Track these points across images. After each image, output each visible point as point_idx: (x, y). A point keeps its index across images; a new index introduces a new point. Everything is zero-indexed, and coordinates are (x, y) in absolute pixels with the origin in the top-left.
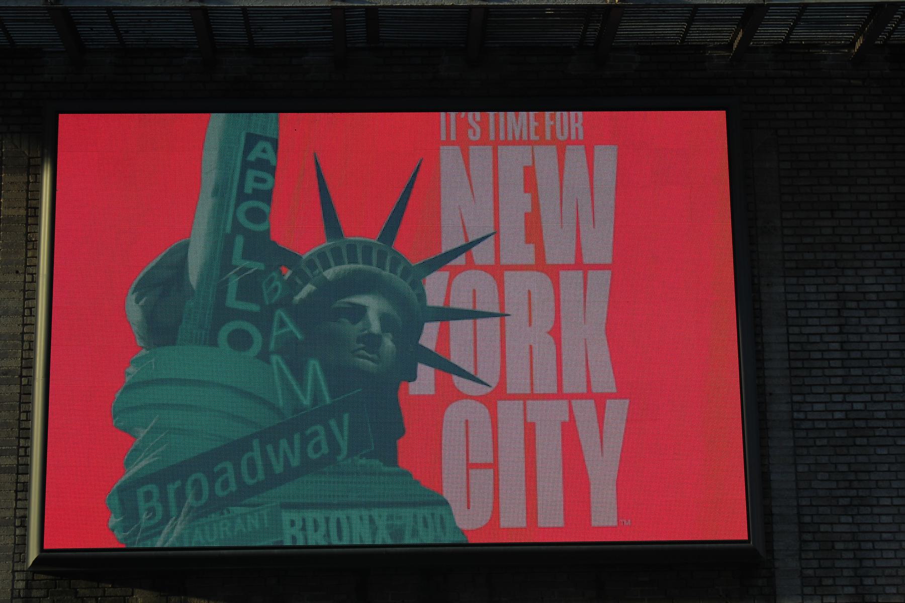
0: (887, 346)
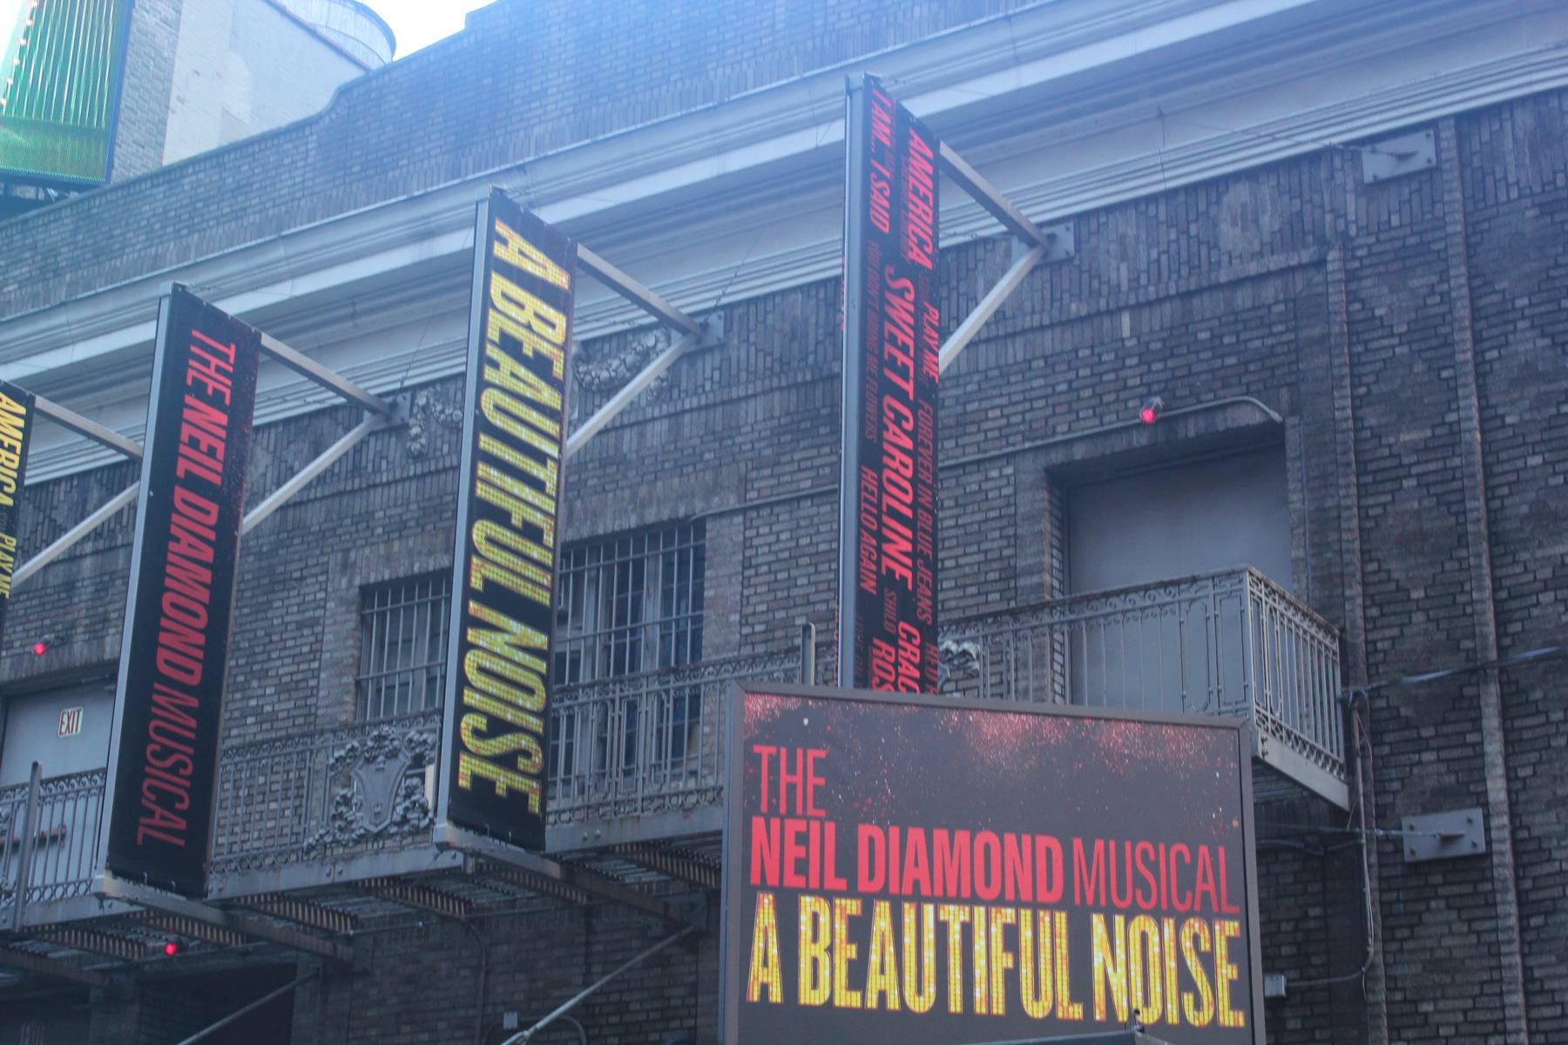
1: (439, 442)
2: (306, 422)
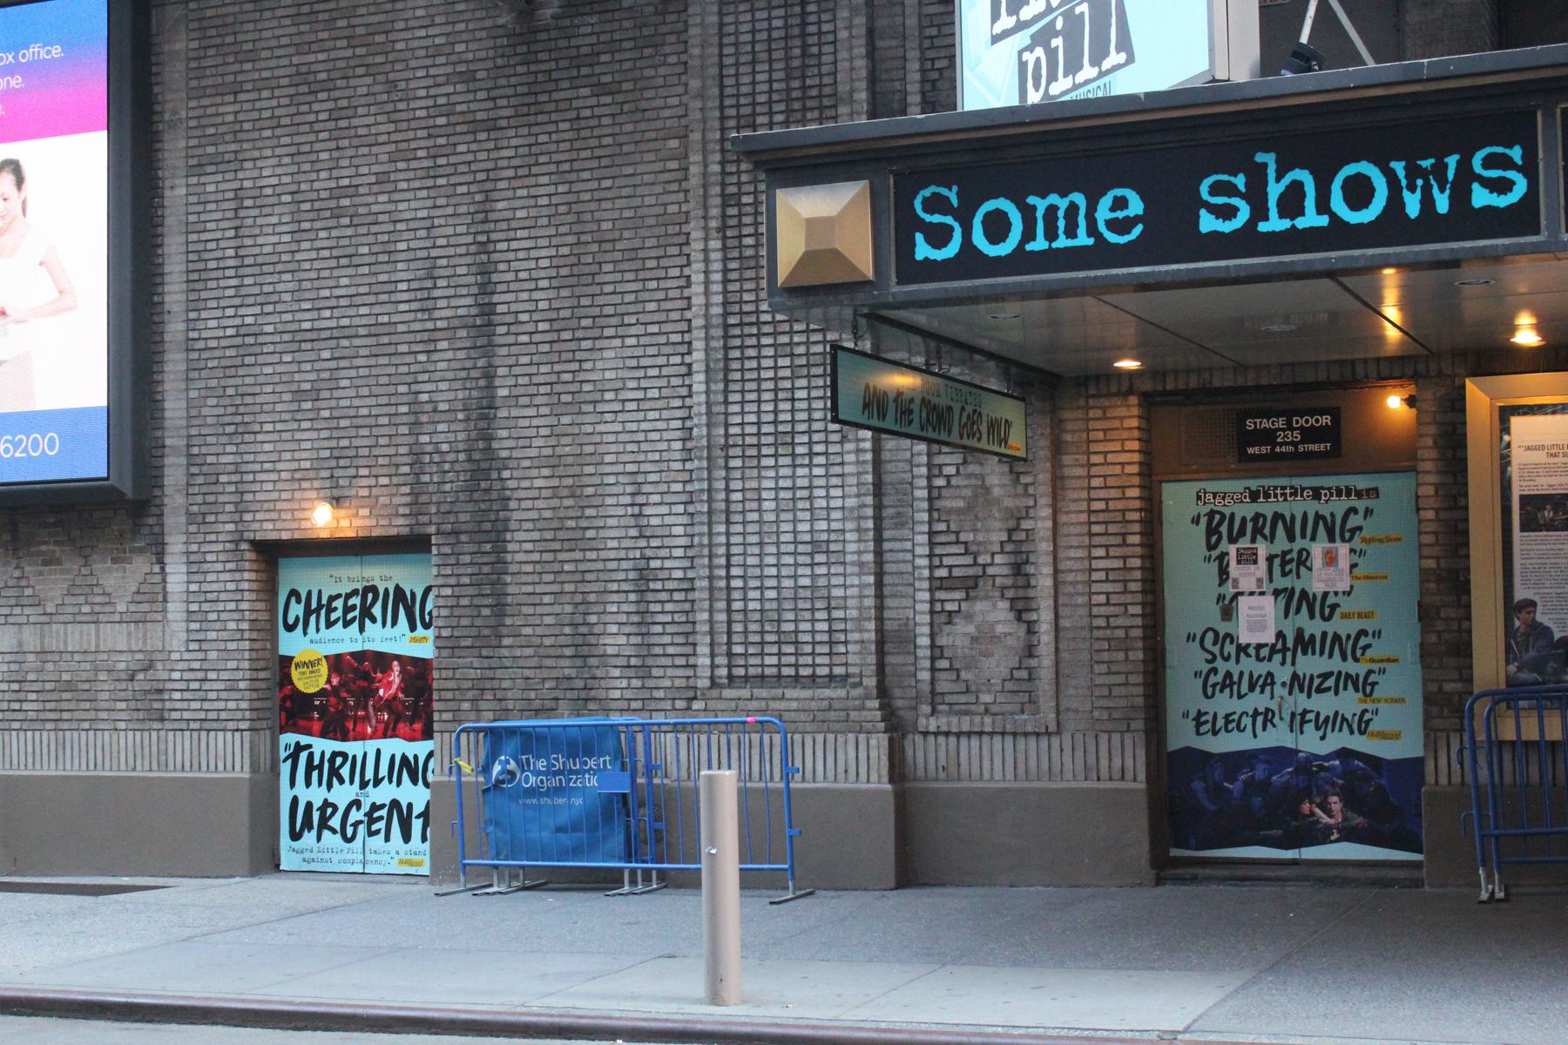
0: (280, 248)
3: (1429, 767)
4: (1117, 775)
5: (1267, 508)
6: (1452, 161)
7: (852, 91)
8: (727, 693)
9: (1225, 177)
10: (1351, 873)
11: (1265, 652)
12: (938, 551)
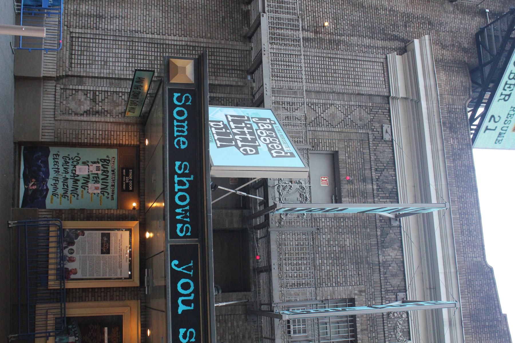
1: (391, 322)
2: (402, 269)
3: (43, 210)
4: (43, 134)
5: (110, 174)
6: (188, 220)
7: (218, 80)
8: (68, 36)
9: (188, 168)
10: (16, 191)
11: (74, 172)
12: (103, 93)
